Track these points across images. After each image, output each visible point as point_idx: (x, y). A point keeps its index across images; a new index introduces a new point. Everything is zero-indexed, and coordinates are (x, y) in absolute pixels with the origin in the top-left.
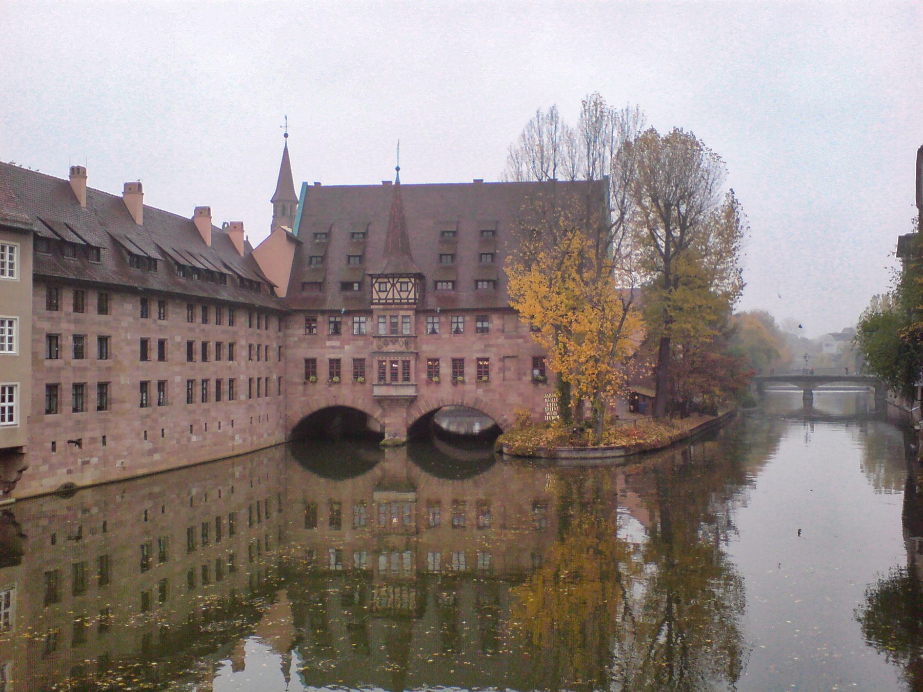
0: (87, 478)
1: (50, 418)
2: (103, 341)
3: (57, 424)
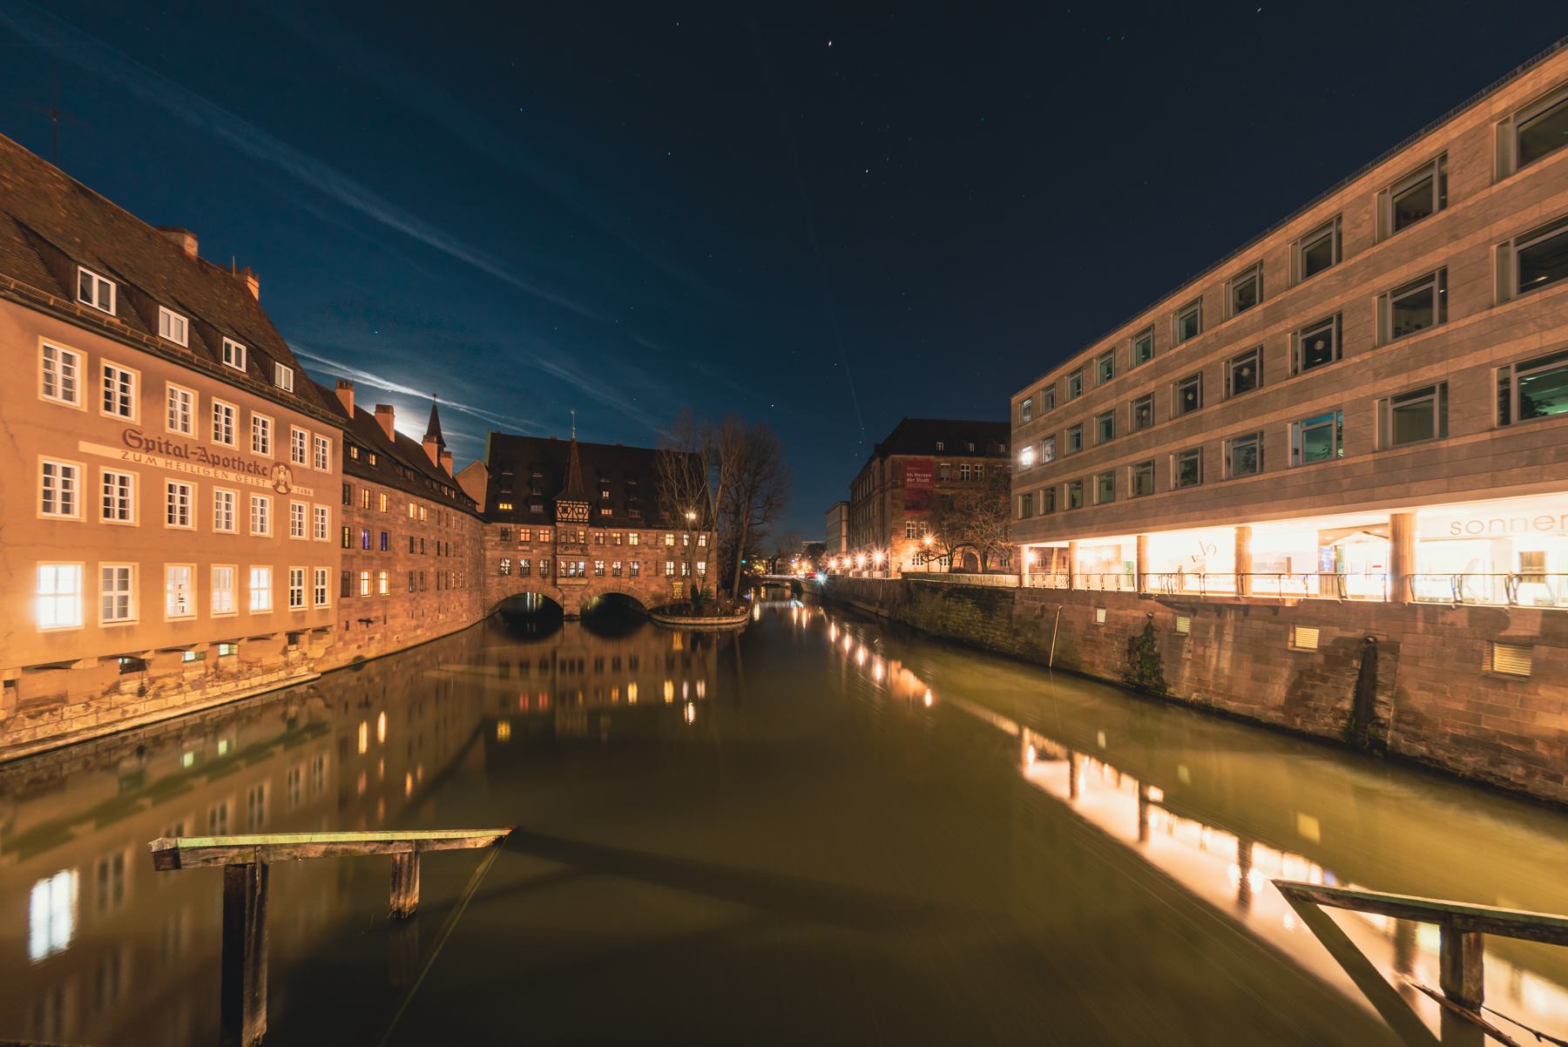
0: (371, 652)
1: (345, 601)
2: (384, 536)
3: (350, 606)
